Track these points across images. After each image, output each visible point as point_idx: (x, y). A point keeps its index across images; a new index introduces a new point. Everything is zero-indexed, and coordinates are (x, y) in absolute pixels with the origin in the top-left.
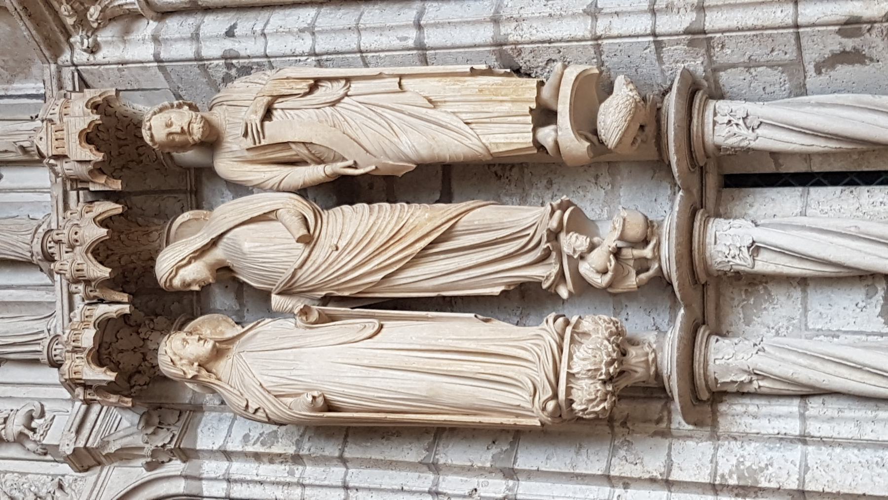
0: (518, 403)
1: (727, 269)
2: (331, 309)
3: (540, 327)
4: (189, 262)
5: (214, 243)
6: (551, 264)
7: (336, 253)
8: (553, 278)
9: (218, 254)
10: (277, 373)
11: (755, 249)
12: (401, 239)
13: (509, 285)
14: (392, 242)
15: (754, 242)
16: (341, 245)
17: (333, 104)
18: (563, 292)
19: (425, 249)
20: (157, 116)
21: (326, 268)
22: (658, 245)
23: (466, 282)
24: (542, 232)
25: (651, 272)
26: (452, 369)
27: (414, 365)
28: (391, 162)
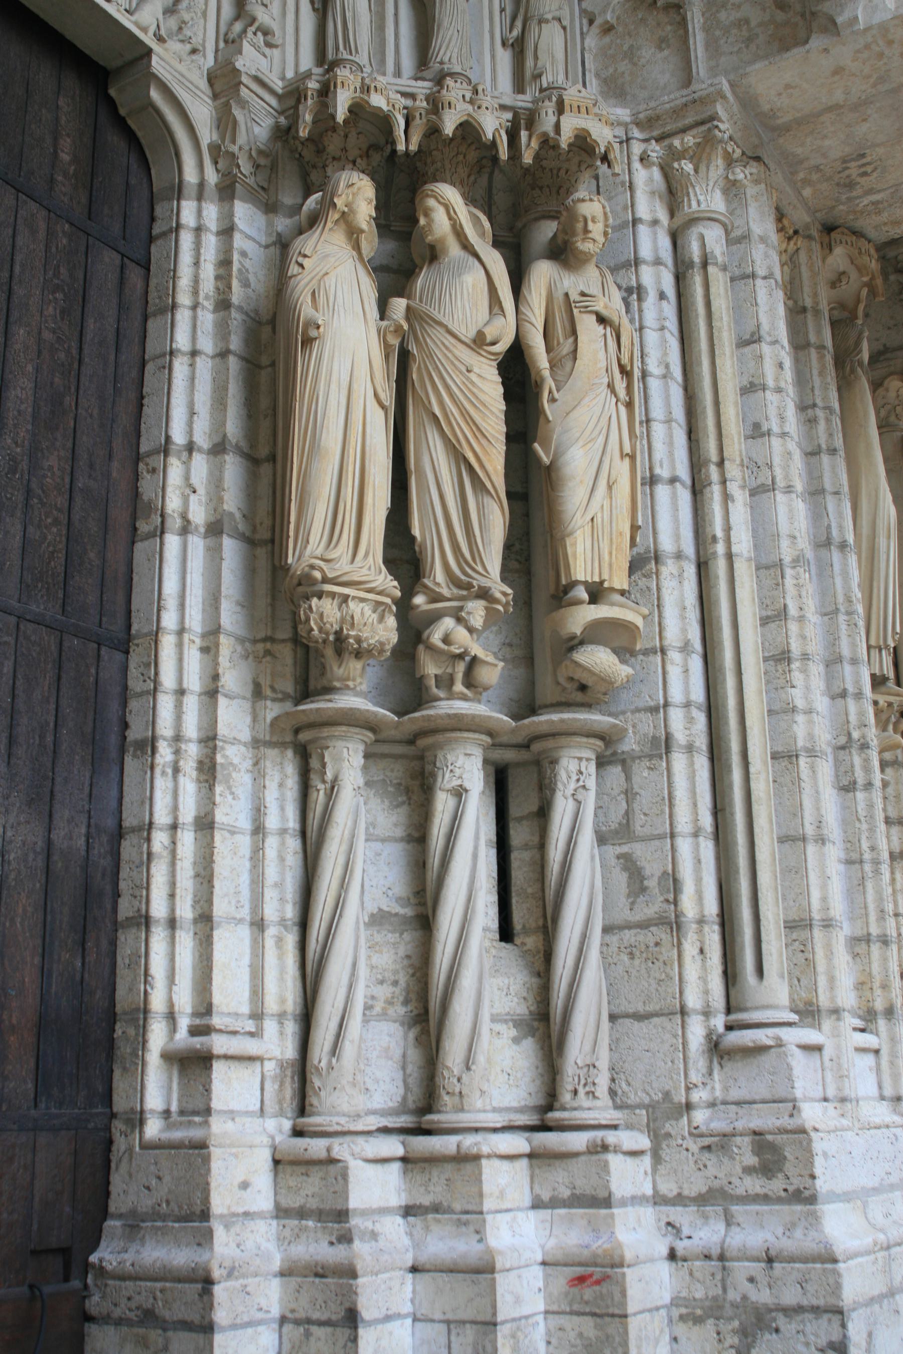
1: (438, 764)
4: (450, 218)
7: (464, 370)
9: (454, 250)
10: (339, 293)
11: (460, 793)
13: (423, 546)
15: (466, 791)
16: (472, 376)
21: (448, 358)
22: (464, 698)
23: (428, 502)
25: (435, 690)
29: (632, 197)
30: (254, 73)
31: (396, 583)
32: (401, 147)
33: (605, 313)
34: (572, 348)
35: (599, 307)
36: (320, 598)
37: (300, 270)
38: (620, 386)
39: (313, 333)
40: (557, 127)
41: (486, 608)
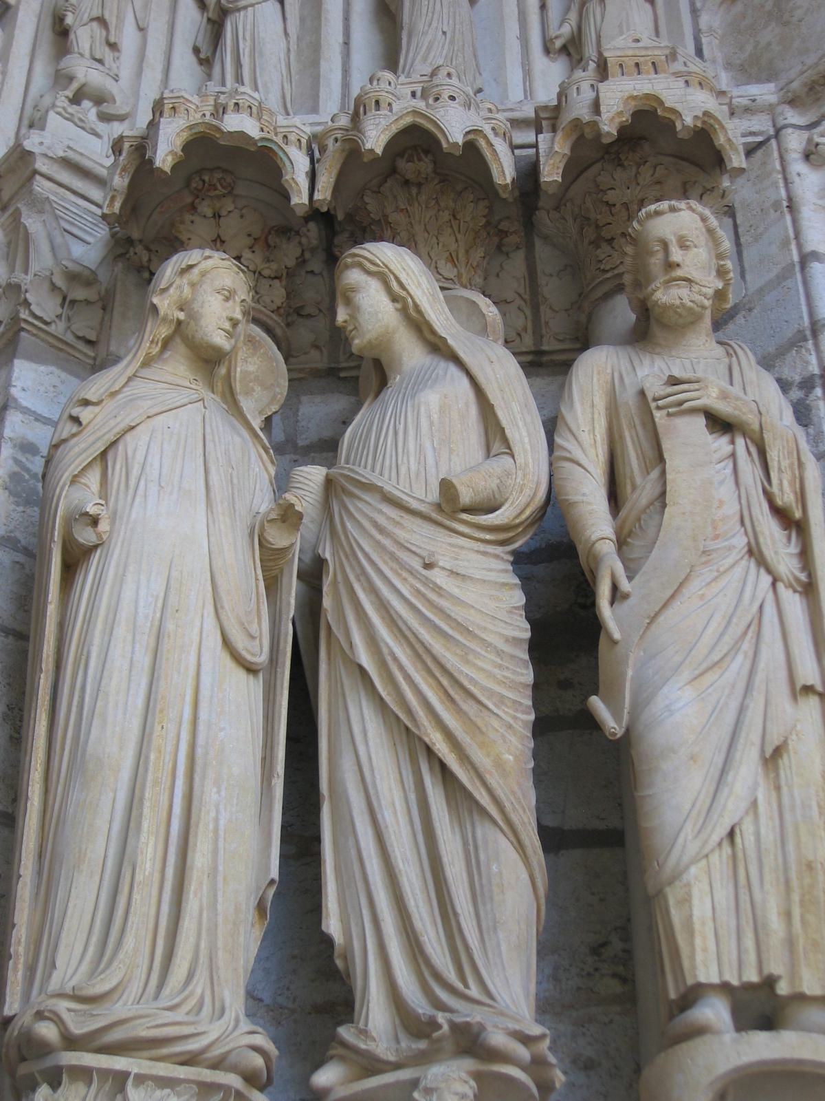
0: (59, 963)
2: (292, 589)
3: (242, 1017)
4: (395, 298)
5: (438, 347)
6: (398, 1041)
7: (416, 564)
8: (363, 1046)
12: (452, 700)
13: (347, 956)
14: (445, 682)
16: (438, 576)
17: (755, 552)
18: (326, 1077)
19: (429, 751)
20: (700, 224)
23: (353, 852)
24: (475, 1016)
26: (146, 811)
27: (158, 728)
28: (630, 673)
29: (795, 222)
30: (61, 154)
31: (260, 1040)
32: (300, 198)
33: (723, 408)
34: (658, 491)
35: (711, 398)
36: (55, 1084)
37: (75, 429)
38: (781, 550)
39: (85, 536)
40: (596, 106)
41: (478, 1076)
